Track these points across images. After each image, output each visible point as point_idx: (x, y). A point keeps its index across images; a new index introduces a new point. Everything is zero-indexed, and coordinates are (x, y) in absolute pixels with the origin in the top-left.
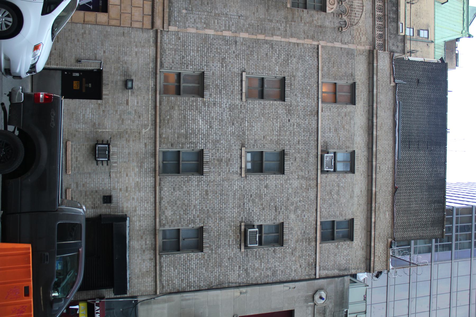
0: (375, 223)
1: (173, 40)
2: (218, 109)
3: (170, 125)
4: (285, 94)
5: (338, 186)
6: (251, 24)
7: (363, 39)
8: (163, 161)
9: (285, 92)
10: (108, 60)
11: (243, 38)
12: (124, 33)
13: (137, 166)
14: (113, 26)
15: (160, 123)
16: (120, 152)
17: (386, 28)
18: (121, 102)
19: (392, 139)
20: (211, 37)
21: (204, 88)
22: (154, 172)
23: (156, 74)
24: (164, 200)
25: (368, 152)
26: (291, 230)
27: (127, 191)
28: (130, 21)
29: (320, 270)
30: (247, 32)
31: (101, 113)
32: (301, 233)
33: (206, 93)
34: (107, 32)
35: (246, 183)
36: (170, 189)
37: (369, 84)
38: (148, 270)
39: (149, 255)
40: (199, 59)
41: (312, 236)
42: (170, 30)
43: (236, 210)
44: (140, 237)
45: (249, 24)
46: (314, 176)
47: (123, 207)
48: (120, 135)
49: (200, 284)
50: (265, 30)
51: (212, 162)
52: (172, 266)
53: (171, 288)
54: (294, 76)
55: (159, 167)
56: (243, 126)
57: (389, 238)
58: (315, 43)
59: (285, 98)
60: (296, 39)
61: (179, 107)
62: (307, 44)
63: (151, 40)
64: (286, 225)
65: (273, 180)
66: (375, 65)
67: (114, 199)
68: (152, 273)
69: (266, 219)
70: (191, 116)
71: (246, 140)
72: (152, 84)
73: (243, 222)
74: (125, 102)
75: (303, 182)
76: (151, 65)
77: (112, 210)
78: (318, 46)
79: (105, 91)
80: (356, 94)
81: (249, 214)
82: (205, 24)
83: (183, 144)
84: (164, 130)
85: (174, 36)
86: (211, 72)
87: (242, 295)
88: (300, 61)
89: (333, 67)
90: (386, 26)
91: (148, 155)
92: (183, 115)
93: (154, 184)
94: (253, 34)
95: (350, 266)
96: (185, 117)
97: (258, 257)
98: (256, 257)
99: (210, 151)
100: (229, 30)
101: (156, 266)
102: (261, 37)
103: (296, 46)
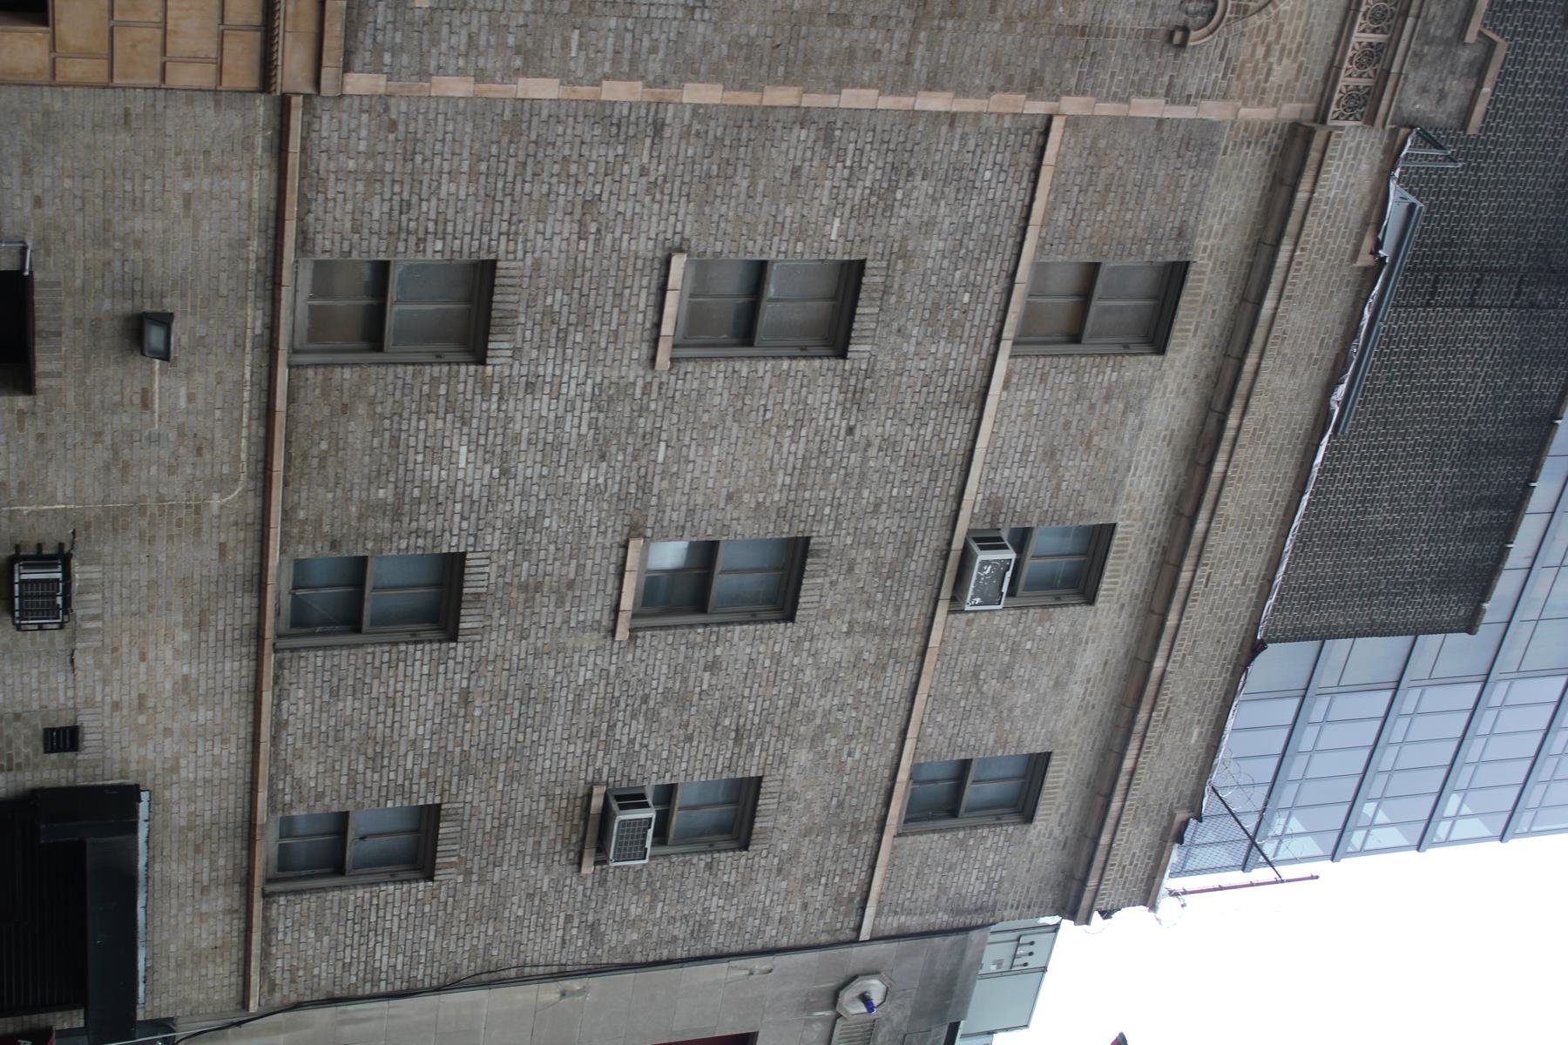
0: (1133, 772)
1: (364, 133)
2: (543, 405)
3: (331, 471)
4: (850, 329)
5: (1014, 650)
6: (743, 40)
7: (1282, 71)
8: (295, 588)
9: (851, 320)
10: (53, 235)
11: (695, 108)
12: (127, 114)
13: (186, 625)
14: (75, 85)
15: (287, 468)
16: (112, 582)
17: (1410, 21)
18: (117, 398)
19: (1292, 474)
20: (545, 113)
21: (487, 326)
22: (253, 642)
23: (276, 282)
24: (291, 730)
25: (1172, 528)
26: (789, 799)
27: (141, 706)
28: (158, 61)
29: (878, 914)
30: (718, 80)
31: (32, 444)
32: (826, 808)
33: (499, 346)
34: (47, 113)
35: (630, 657)
36: (318, 692)
37: (1251, 266)
38: (219, 943)
39: (221, 901)
40: (479, 208)
41: (870, 811)
42: (348, 90)
43: (578, 748)
44: (191, 848)
45: (734, 44)
46: (917, 623)
47: (125, 761)
48: (116, 520)
49: (414, 973)
50: (808, 63)
51: (500, 594)
52: (312, 925)
53: (302, 990)
54: (905, 256)
55: (278, 613)
56: (643, 462)
57: (1181, 808)
58: (1039, 107)
59: (847, 343)
60: (950, 95)
61: (372, 403)
62: (1000, 116)
63: (259, 140)
64: (768, 786)
65: (743, 644)
66: (1301, 196)
67: (90, 739)
68: (234, 951)
69: (697, 768)
70: (422, 436)
71: (653, 511)
72: (259, 323)
73: (598, 784)
74: (137, 399)
75: (870, 649)
76: (256, 247)
77: (80, 771)
78: (1049, 119)
79: (44, 362)
80: (1180, 313)
81: (629, 756)
82: (518, 53)
83: (379, 539)
84: (304, 495)
85: (365, 117)
86: (529, 261)
87: (566, 1000)
88: (950, 192)
89: (1102, 207)
90: (1413, 11)
91: (230, 586)
92: (387, 435)
93: (251, 680)
94: (744, 87)
95: (1001, 897)
96: (395, 442)
97: (643, 886)
98: (637, 886)
99: (494, 557)
100: (629, 77)
101: (248, 931)
102: (782, 96)
103: (944, 129)
